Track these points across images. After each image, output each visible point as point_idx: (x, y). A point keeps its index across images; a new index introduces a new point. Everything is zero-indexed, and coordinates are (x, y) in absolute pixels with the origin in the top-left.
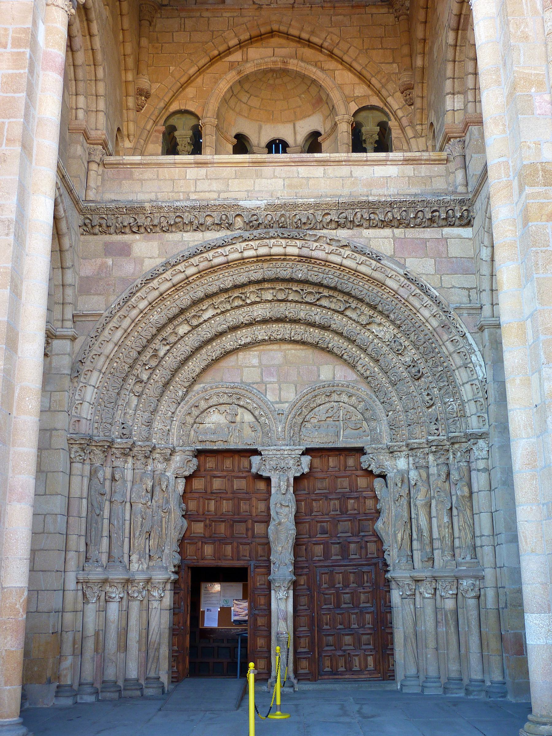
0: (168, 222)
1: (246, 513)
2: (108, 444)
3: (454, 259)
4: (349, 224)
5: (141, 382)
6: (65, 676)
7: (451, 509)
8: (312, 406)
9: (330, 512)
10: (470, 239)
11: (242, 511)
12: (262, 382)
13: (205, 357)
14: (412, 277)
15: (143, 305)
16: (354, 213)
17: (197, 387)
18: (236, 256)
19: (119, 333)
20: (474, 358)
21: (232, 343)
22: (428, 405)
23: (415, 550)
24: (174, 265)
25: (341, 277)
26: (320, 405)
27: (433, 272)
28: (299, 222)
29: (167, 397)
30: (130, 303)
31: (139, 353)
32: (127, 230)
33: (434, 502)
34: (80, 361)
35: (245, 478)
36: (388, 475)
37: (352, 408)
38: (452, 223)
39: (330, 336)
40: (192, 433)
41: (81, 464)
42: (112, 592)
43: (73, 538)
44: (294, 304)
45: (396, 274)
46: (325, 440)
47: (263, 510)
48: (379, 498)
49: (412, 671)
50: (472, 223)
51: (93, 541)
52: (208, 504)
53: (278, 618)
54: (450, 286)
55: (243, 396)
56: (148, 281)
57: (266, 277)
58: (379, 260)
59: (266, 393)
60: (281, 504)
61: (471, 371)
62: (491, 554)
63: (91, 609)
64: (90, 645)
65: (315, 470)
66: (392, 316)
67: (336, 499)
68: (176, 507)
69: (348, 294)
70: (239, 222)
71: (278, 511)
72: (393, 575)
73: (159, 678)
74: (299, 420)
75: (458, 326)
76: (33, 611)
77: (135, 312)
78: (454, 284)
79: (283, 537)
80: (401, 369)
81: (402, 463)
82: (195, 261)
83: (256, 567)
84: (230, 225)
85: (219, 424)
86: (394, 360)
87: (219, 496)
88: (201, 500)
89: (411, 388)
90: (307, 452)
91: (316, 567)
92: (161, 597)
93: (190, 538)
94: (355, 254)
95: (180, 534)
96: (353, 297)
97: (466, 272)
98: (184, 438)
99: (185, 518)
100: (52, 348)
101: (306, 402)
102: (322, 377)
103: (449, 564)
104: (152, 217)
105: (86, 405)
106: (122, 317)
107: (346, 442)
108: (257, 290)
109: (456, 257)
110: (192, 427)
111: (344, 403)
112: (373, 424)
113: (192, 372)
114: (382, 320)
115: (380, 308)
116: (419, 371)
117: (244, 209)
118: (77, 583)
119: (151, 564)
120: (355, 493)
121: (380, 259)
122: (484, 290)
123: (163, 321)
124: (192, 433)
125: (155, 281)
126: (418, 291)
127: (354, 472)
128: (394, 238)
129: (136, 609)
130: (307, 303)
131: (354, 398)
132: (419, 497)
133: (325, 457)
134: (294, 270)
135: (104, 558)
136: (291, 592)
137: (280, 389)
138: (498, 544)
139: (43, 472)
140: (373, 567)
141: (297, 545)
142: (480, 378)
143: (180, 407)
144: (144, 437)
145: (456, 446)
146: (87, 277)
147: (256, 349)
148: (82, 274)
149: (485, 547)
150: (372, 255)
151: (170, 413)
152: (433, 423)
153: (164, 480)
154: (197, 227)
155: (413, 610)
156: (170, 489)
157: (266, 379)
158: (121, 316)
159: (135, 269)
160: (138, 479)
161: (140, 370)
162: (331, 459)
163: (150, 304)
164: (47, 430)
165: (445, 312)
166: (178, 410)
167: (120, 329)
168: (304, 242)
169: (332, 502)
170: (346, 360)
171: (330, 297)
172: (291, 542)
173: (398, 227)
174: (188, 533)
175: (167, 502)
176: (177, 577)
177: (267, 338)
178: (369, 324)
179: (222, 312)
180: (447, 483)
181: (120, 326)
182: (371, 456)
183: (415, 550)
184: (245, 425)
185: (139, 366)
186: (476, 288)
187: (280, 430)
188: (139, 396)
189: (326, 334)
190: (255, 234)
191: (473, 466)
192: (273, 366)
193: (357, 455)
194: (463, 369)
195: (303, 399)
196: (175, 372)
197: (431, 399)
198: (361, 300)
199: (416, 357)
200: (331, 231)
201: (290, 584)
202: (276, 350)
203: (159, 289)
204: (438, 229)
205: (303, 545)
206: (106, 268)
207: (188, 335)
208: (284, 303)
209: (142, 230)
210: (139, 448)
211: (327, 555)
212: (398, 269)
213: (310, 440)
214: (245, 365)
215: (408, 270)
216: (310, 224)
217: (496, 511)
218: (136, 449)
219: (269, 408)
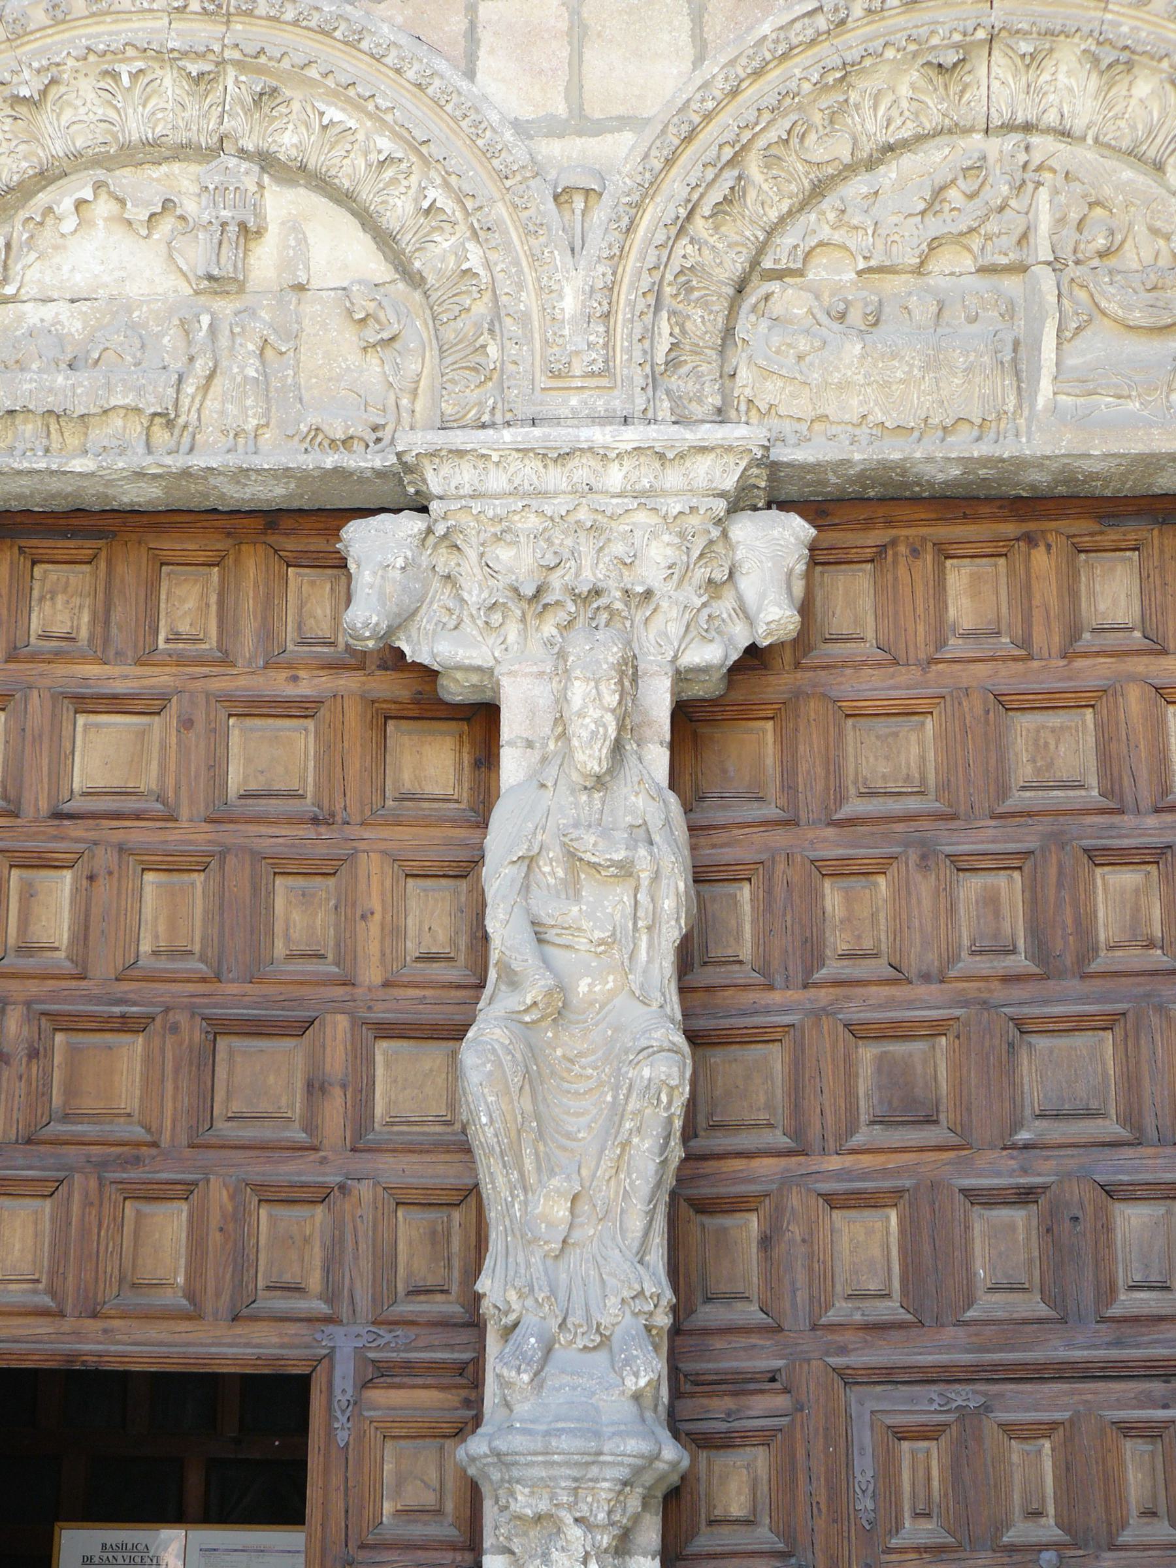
1: (312, 967)
8: (819, 154)
9: (952, 958)
11: (280, 949)
35: (304, 709)
47: (439, 942)
52: (28, 894)
67: (1005, 862)
71: (549, 909)
85: (120, 306)
91: (848, 1378)
111: (1064, 134)
120: (1152, 821)
127: (1139, 665)
133: (915, 553)
162: (958, 576)
169: (971, 887)
184: (310, 308)
201: (634, 1503)
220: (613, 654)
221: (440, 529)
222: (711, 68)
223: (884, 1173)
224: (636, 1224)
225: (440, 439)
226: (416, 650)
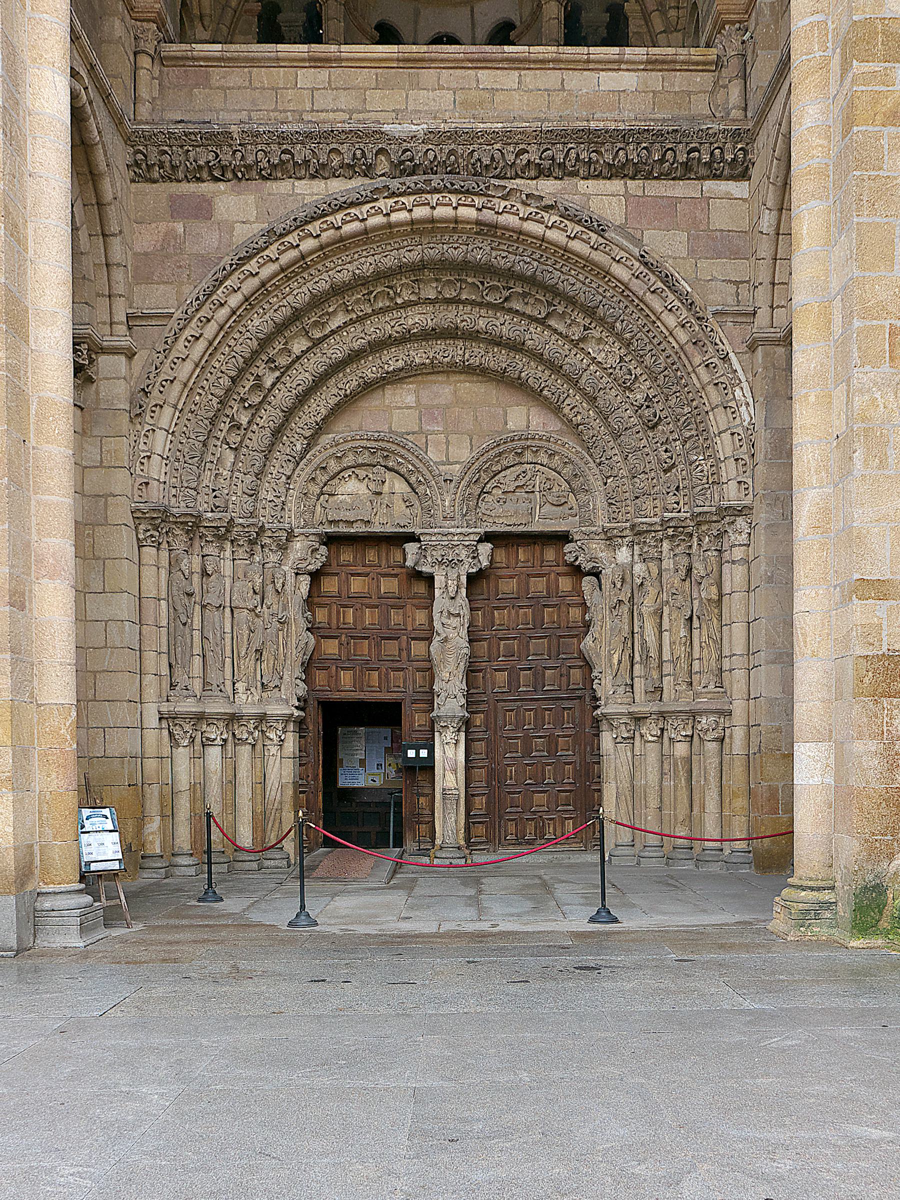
0: (269, 161)
4: (557, 170)
8: (494, 469)
12: (421, 431)
15: (234, 300)
16: (566, 150)
17: (325, 439)
19: (201, 345)
21: (374, 368)
28: (479, 164)
29: (278, 453)
30: (214, 297)
31: (233, 380)
35: (396, 575)
36: (603, 571)
37: (554, 473)
39: (524, 360)
40: (318, 508)
44: (469, 308)
45: (628, 255)
46: (513, 520)
58: (601, 232)
59: (427, 448)
69: (553, 291)
70: (383, 165)
71: (445, 621)
77: (224, 312)
80: (628, 411)
84: (370, 167)
86: (619, 397)
87: (358, 601)
89: (643, 441)
90: (488, 537)
94: (565, 221)
96: (559, 295)
98: (307, 516)
101: (486, 462)
102: (511, 425)
104: (243, 151)
105: (155, 458)
106: (204, 320)
107: (543, 524)
108: (413, 281)
111: (542, 465)
113: (316, 414)
114: (604, 333)
117: (391, 139)
121: (603, 230)
123: (267, 329)
124: (318, 508)
125: (253, 262)
130: (489, 306)
136: (462, 735)
137: (448, 443)
143: (298, 468)
144: (246, 511)
150: (592, 222)
158: (202, 319)
159: (220, 242)
161: (235, 408)
163: (247, 300)
166: (296, 473)
167: (201, 339)
170: (546, 398)
171: (524, 295)
178: (583, 339)
181: (201, 335)
184: (395, 497)
185: (233, 402)
188: (236, 449)
189: (517, 357)
192: (438, 407)
196: (289, 414)
198: (571, 301)
200: (529, 181)
202: (442, 383)
205: (480, 671)
207: (307, 355)
211: (514, 682)
212: (631, 247)
214: (395, 404)
216: (496, 168)
221: (423, 547)
222: (473, 454)
223: (504, 665)
225: (422, 531)
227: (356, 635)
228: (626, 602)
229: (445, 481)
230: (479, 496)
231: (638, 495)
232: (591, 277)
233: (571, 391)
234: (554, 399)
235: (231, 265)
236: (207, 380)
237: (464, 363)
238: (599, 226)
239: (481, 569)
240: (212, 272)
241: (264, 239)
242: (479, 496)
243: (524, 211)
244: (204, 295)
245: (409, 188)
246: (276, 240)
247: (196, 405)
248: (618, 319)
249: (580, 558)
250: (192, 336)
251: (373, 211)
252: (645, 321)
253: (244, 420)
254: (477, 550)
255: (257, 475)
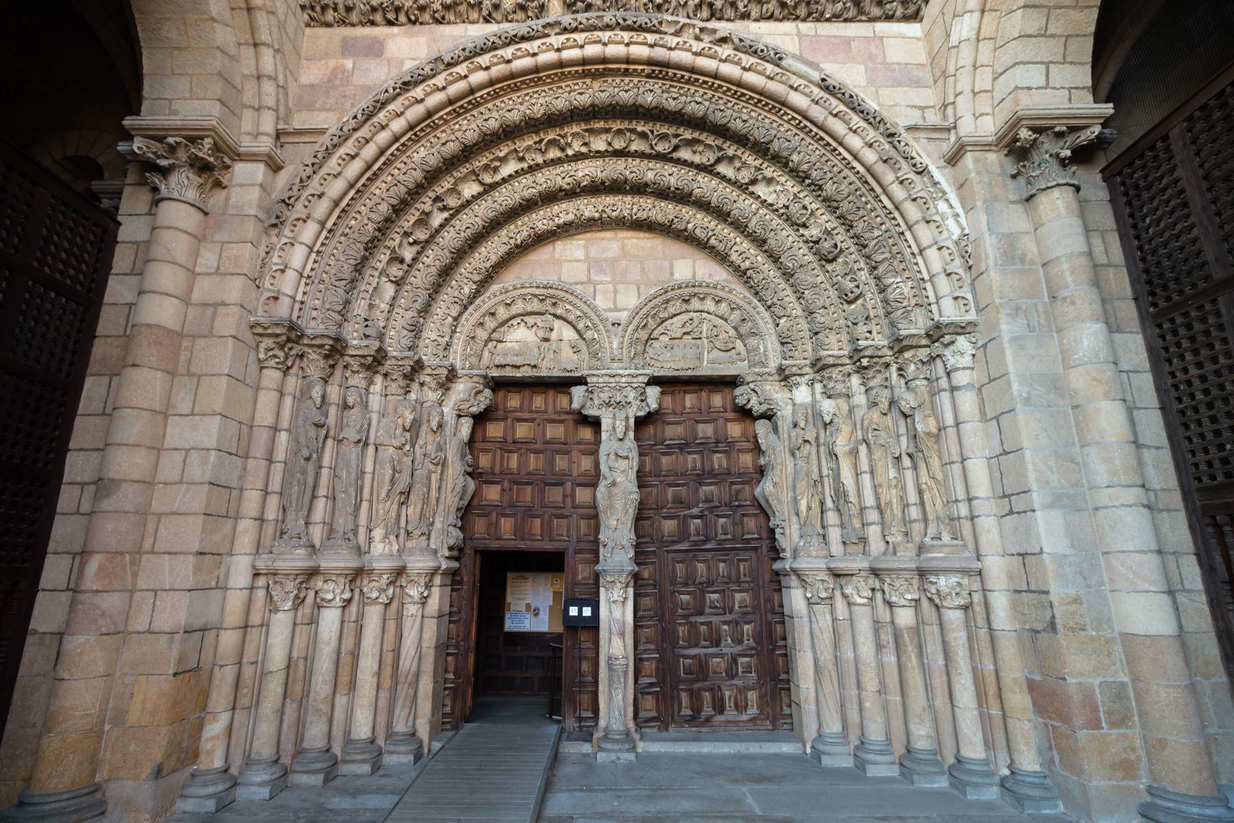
2: (331, 342)
3: (896, 67)
5: (402, 261)
6: (210, 753)
7: (898, 459)
8: (661, 316)
10: (918, 39)
13: (506, 240)
14: (834, 83)
15: (398, 125)
17: (495, 288)
18: (548, 57)
20: (942, 206)
22: (851, 296)
23: (831, 526)
24: (449, 65)
25: (714, 100)
26: (675, 315)
27: (864, 83)
30: (375, 120)
32: (378, 17)
33: (863, 449)
34: (283, 201)
35: (561, 422)
36: (779, 413)
37: (720, 320)
38: (891, 13)
40: (486, 354)
41: (278, 371)
42: (328, 591)
43: (252, 498)
44: (638, 160)
45: (806, 83)
48: (763, 448)
49: (833, 726)
50: (921, 13)
51: (294, 504)
53: (611, 633)
54: (892, 103)
55: (561, 300)
56: (407, 86)
57: (597, 102)
59: (595, 296)
60: (617, 455)
61: (938, 227)
62: (995, 531)
63: (281, 623)
64: (274, 688)
65: (664, 411)
66: (795, 157)
67: (696, 453)
68: (457, 460)
69: (722, 131)
71: (612, 464)
72: (796, 565)
73: (414, 734)
74: (643, 335)
75: (914, 154)
76: (140, 629)
78: (897, 100)
79: (619, 505)
81: (802, 394)
82: (484, 60)
83: (578, 551)
86: (790, 238)
88: (499, 452)
90: (654, 381)
92: (426, 598)
93: (480, 507)
94: (740, 55)
95: (461, 499)
97: (916, 83)
98: (474, 360)
99: (472, 478)
100: (232, 176)
103: (901, 548)
105: (291, 275)
106: (362, 140)
107: (712, 369)
109: (899, 64)
110: (485, 345)
111: (709, 313)
112: (752, 342)
115: (775, 146)
116: (836, 246)
118: (256, 575)
119: (409, 544)
122: (960, 93)
123: (434, 161)
126: (842, 107)
127: (722, 414)
128: (799, 34)
129: (375, 617)
131: (724, 305)
132: (838, 442)
134: (641, 90)
135: (317, 533)
136: (631, 591)
137: (615, 292)
138: (1011, 512)
139: (194, 375)
140: (753, 553)
141: (639, 518)
142: (955, 237)
145: (908, 355)
146: (312, 86)
147: (581, 236)
148: (304, 80)
149: (983, 518)
151: (450, 319)
152: (861, 324)
153: (435, 414)
154: (490, 15)
155: (830, 623)
156: (448, 430)
157: (594, 278)
160: (391, 410)
161: (398, 241)
164: (208, 305)
165: (892, 135)
166: (466, 315)
167: (357, 159)
168: (657, 36)
172: (631, 512)
173: (804, 20)
174: (475, 503)
175: (440, 448)
176: (456, 564)
177: (597, 215)
178: (754, 182)
179: (533, 169)
180: (889, 417)
181: (357, 155)
182: (752, 385)
183: (831, 526)
184: (563, 344)
185: (396, 235)
186: (933, 107)
187: (615, 346)
190: (579, 19)
191: (944, 383)
193: (727, 391)
194: (923, 224)
195: (649, 304)
197: (858, 287)
198: (741, 140)
199: (829, 226)
202: (610, 239)
203: (425, 103)
204: (867, 24)
206: (343, 73)
208: (623, 159)
209: (402, 18)
210: (394, 362)
213: (659, 365)
215: (827, 73)
217: (1005, 453)
218: (389, 362)
219: (598, 316)
220: (624, 415)
224: (629, 525)
226: (585, 412)
227: (518, 481)
228: (813, 442)
229: (613, 324)
230: (647, 341)
231: (818, 330)
232: (764, 113)
233: (738, 239)
234: (721, 247)
235: (394, 89)
236: (365, 205)
237: (631, 216)
238: (776, 54)
239: (649, 413)
240: (374, 93)
241: (431, 66)
242: (647, 341)
243: (697, 46)
244: (363, 114)
245: (581, 23)
246: (445, 70)
247: (350, 228)
248: (793, 151)
249: (752, 402)
250: (347, 155)
251: (544, 47)
252: (823, 151)
253: (408, 254)
254: (645, 392)
255: (419, 312)
